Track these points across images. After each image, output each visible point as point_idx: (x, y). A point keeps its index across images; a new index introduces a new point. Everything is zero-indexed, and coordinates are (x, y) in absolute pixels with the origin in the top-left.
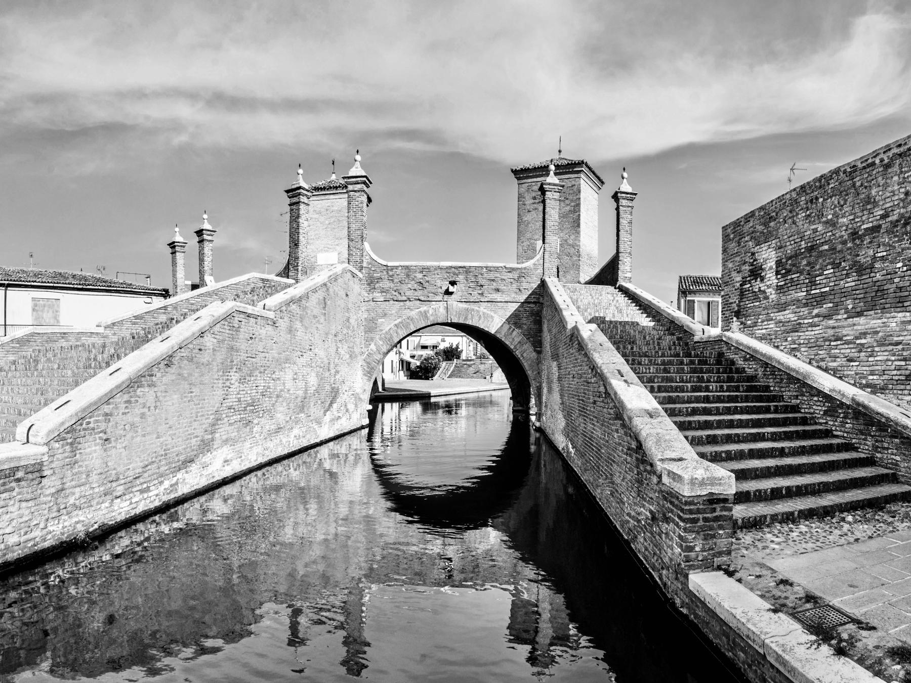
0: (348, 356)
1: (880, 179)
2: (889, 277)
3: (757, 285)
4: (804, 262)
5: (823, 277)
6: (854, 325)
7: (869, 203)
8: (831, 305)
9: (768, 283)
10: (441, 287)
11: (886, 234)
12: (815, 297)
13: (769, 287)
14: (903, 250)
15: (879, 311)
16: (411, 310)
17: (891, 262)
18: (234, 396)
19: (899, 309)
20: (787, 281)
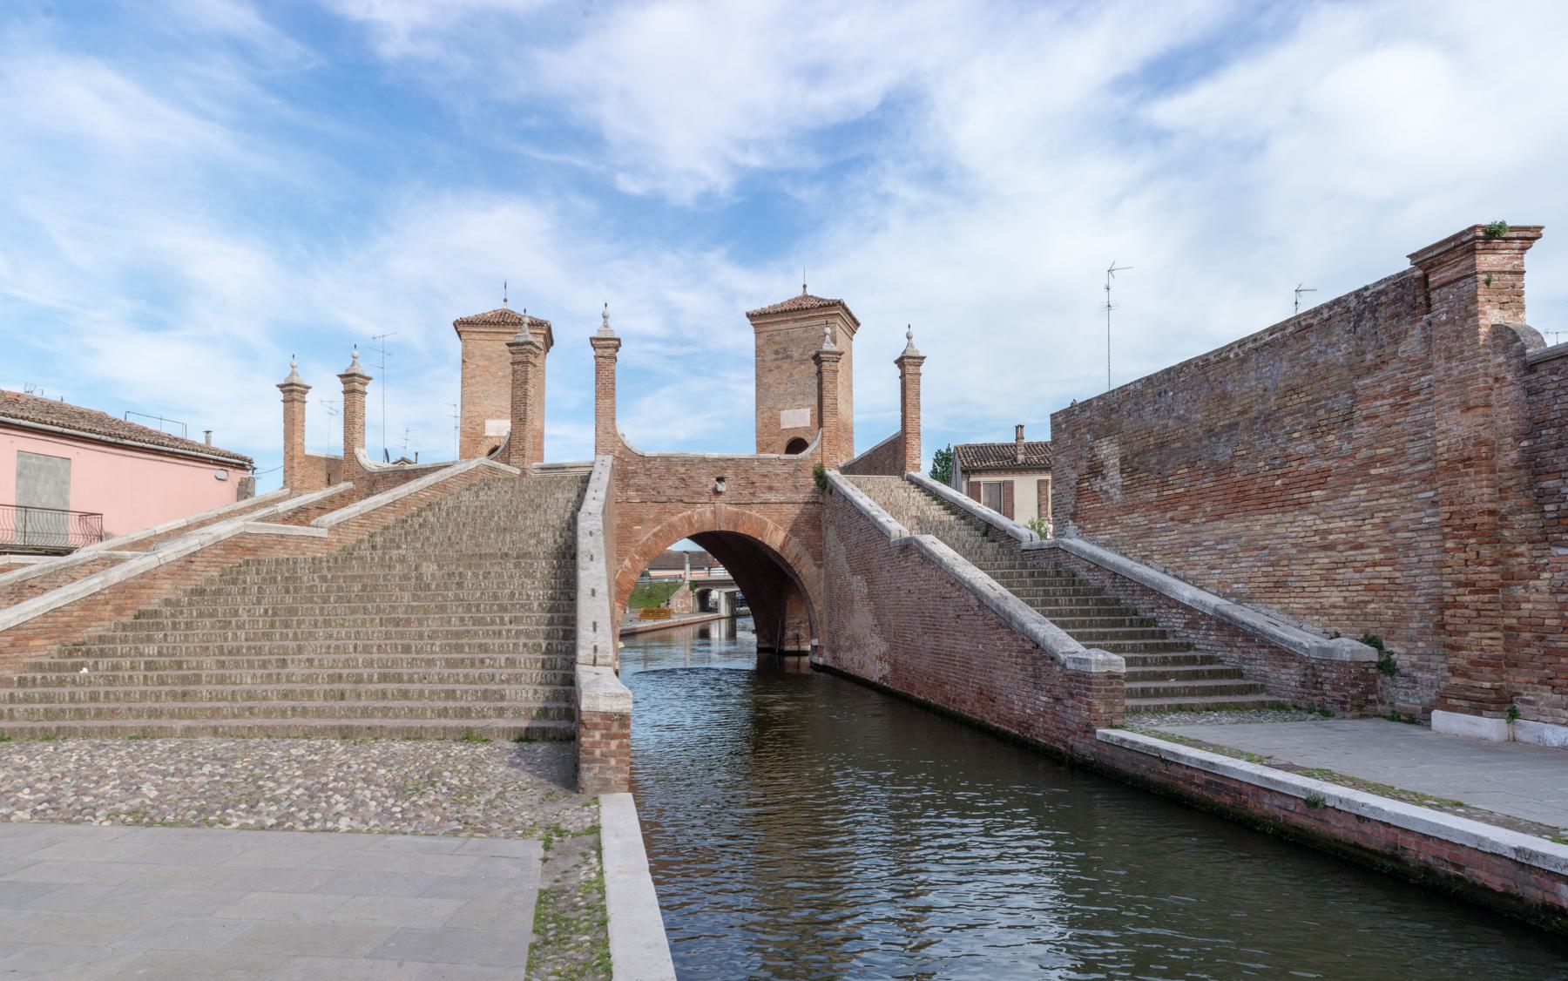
2: (1251, 477)
3: (1098, 484)
4: (1154, 460)
5: (1177, 477)
6: (1214, 529)
8: (1187, 507)
9: (1111, 482)
10: (707, 485)
12: (1168, 498)
13: (1112, 486)
16: (673, 514)
17: (1252, 461)
19: (1263, 511)
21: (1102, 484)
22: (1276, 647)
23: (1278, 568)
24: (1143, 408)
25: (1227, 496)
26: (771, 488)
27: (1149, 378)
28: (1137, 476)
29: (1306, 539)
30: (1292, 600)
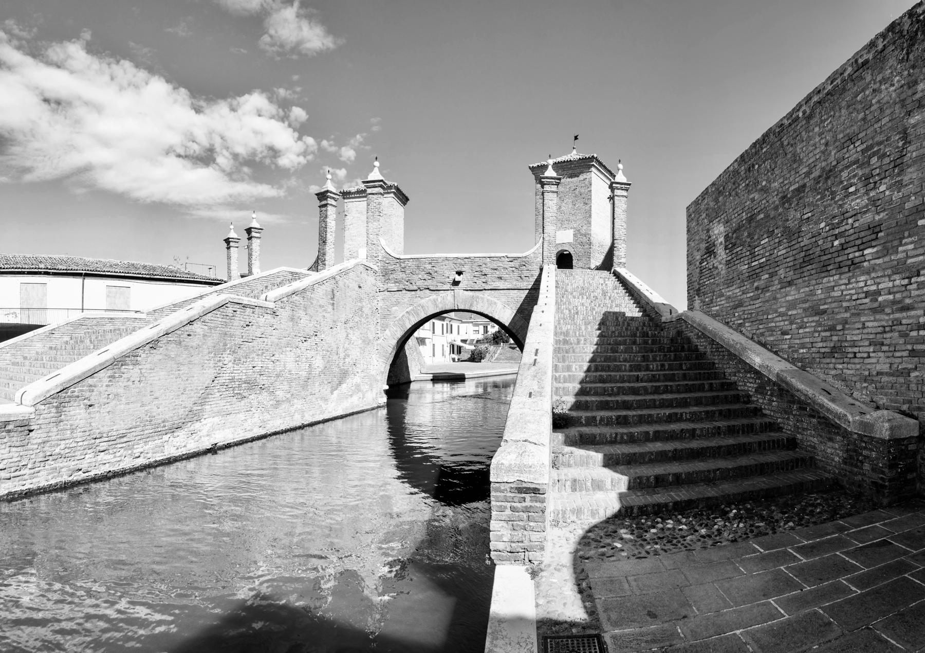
0: (360, 342)
1: (803, 133)
2: (814, 239)
3: (714, 262)
4: (746, 234)
7: (795, 161)
9: (720, 258)
11: (810, 193)
14: (825, 208)
15: (807, 278)
18: (227, 375)
19: (823, 275)
20: (733, 256)
21: (715, 262)
22: (823, 417)
23: (835, 333)
24: (739, 185)
25: (796, 262)
26: (500, 278)
27: (742, 156)
28: (735, 251)
29: (859, 302)
30: (845, 365)
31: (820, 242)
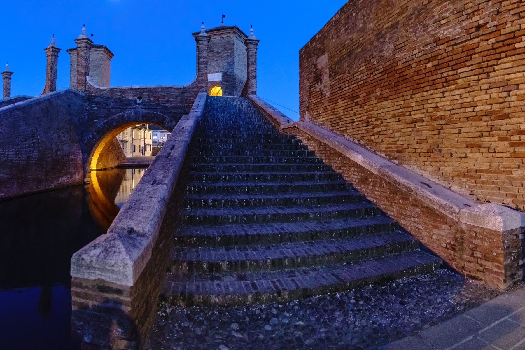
2: (407, 64)
20: (336, 81)
28: (337, 78)
31: (413, 66)
